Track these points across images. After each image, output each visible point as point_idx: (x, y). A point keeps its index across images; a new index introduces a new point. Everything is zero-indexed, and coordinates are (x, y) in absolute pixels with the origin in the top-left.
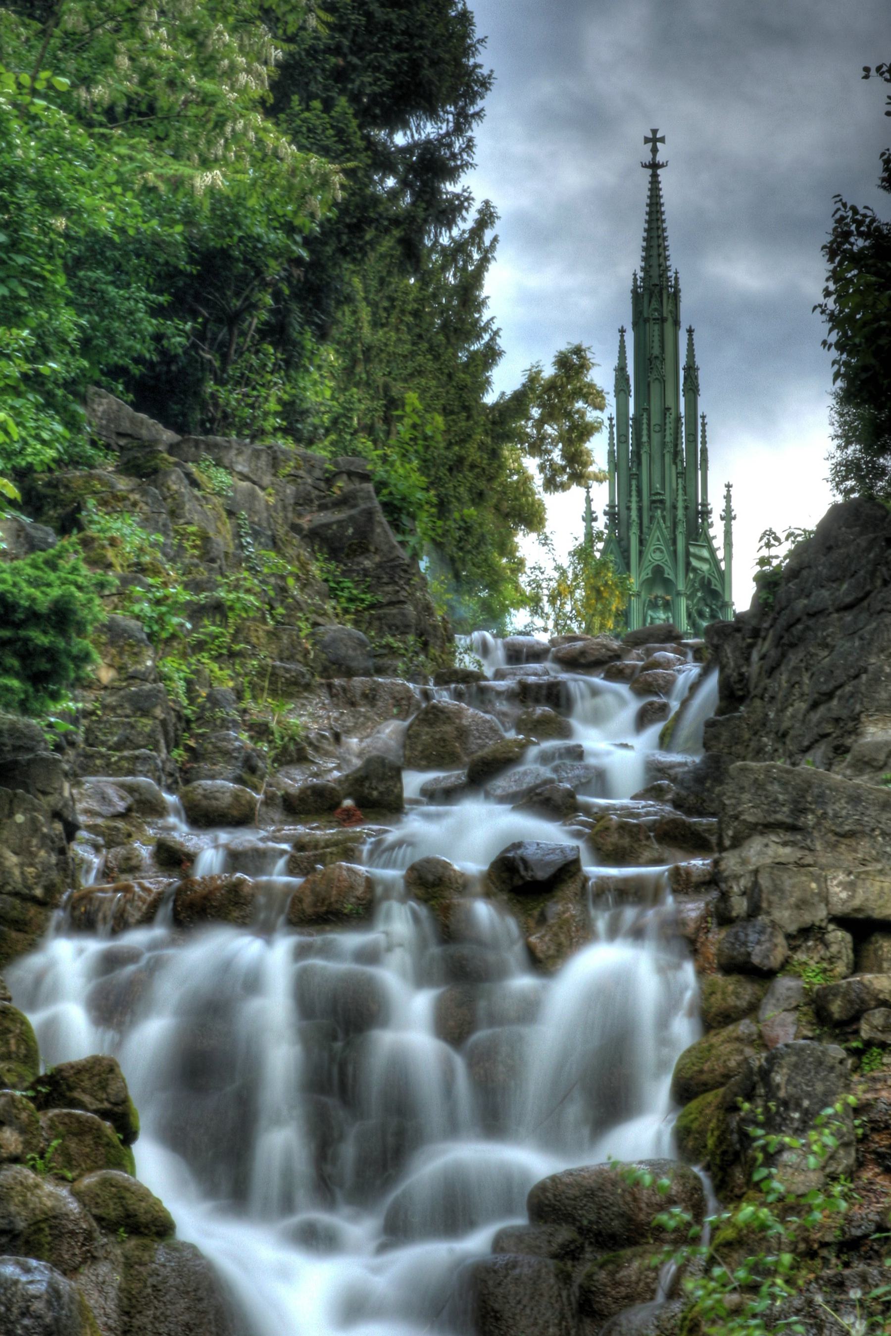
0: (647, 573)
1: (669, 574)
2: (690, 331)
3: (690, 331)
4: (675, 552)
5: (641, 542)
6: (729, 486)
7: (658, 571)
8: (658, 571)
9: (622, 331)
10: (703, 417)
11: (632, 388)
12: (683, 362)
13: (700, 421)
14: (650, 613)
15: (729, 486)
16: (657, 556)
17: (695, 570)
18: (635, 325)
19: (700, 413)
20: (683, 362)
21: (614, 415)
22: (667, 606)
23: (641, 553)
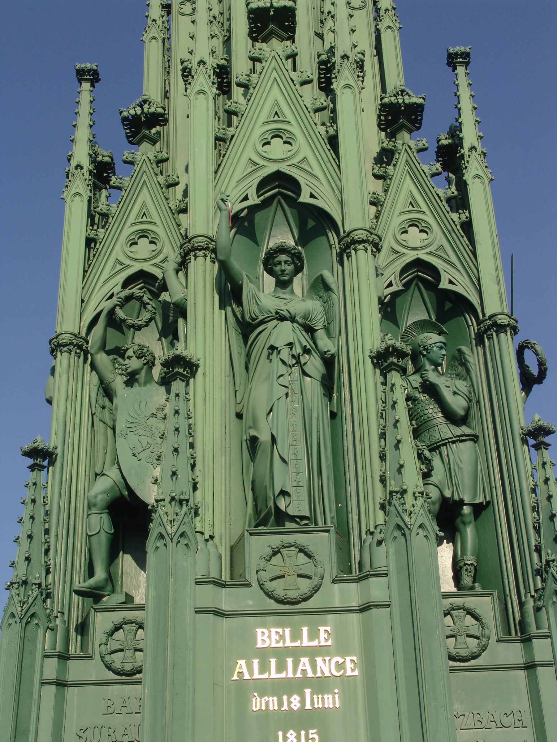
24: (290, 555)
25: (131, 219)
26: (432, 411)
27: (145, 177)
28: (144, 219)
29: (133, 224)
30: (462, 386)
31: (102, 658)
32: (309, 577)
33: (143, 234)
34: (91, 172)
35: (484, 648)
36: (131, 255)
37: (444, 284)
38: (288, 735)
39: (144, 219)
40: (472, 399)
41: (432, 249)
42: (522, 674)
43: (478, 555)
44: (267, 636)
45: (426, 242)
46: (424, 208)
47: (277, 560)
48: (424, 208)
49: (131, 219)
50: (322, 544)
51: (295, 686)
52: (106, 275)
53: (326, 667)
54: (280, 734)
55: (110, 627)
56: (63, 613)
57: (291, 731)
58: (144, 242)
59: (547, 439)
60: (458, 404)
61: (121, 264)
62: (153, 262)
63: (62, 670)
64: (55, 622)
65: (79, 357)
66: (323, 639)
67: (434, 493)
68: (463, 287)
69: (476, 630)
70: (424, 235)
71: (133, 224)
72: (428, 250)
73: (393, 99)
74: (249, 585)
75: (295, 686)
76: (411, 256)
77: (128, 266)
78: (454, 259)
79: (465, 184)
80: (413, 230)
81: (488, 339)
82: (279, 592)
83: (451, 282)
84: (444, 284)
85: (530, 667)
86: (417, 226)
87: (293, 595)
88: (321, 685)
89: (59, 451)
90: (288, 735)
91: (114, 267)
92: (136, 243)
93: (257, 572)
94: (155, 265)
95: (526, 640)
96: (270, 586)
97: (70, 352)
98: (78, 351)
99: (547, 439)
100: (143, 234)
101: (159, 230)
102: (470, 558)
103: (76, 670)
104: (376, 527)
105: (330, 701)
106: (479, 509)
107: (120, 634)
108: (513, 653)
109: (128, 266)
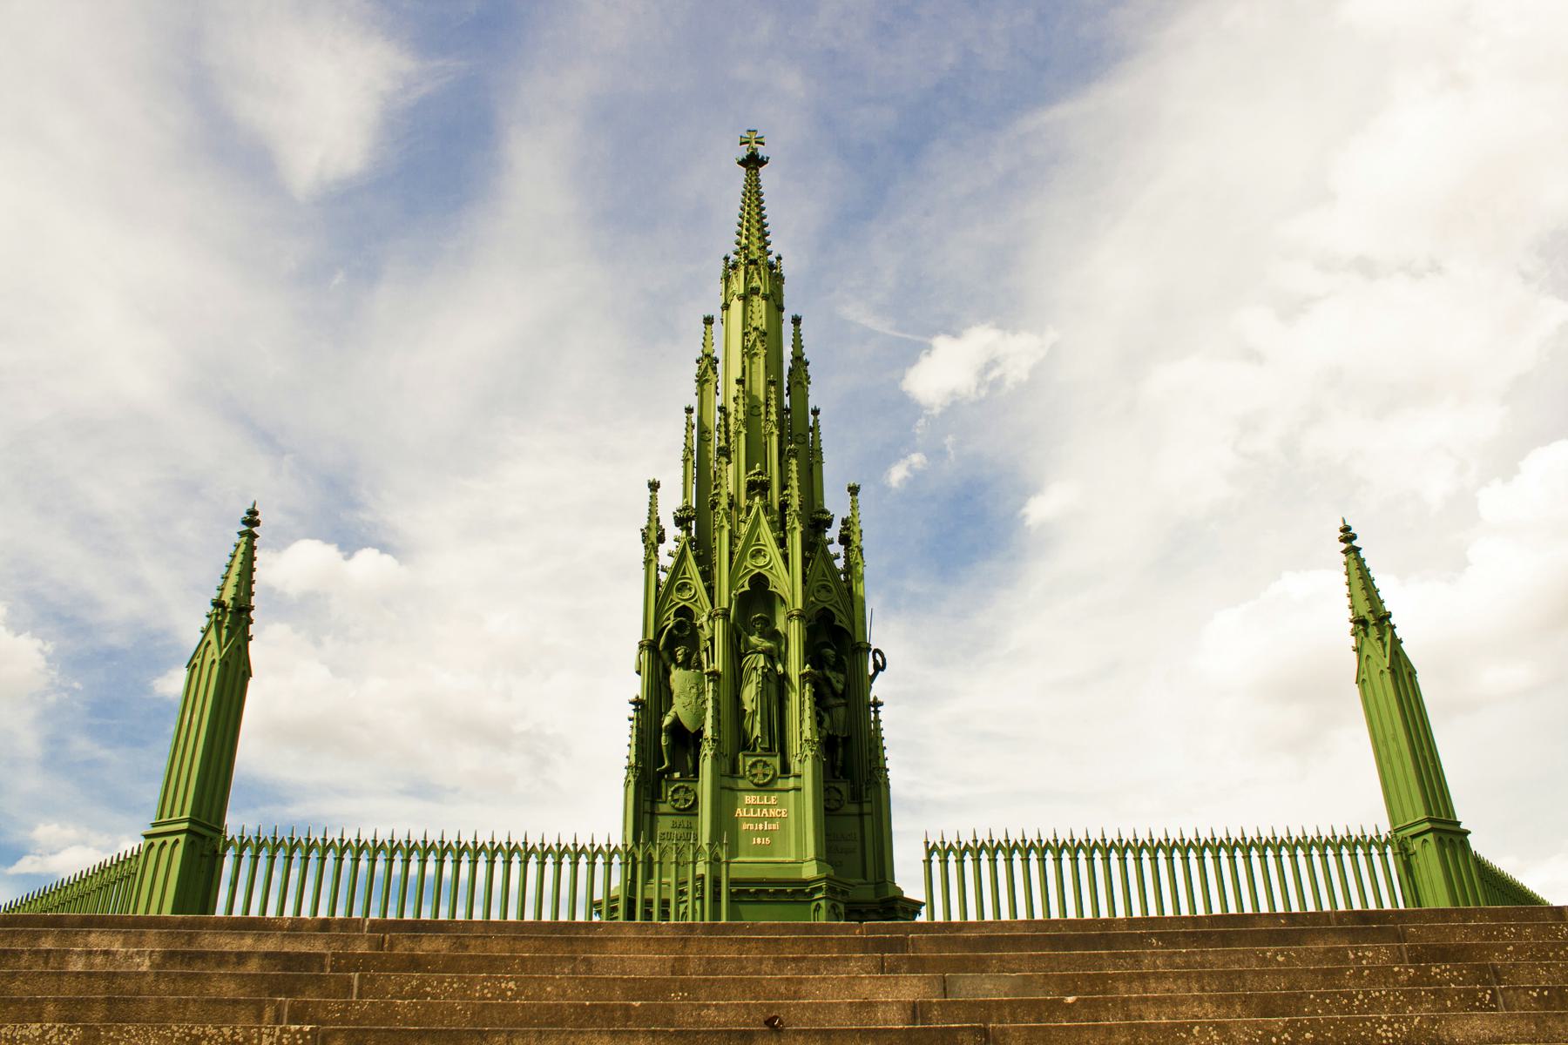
2: (796, 321)
3: (796, 321)
8: (759, 581)
10: (816, 412)
13: (811, 418)
15: (854, 490)
19: (811, 407)
26: (827, 690)
30: (841, 677)
37: (837, 623)
40: (846, 685)
43: (844, 761)
44: (749, 799)
51: (761, 819)
53: (773, 813)
60: (840, 687)
66: (772, 802)
67: (824, 733)
68: (845, 625)
75: (761, 819)
76: (821, 606)
84: (837, 623)
85: (861, 815)
88: (771, 820)
95: (861, 804)
101: (694, 583)
102: (839, 763)
105: (775, 826)
106: (847, 740)
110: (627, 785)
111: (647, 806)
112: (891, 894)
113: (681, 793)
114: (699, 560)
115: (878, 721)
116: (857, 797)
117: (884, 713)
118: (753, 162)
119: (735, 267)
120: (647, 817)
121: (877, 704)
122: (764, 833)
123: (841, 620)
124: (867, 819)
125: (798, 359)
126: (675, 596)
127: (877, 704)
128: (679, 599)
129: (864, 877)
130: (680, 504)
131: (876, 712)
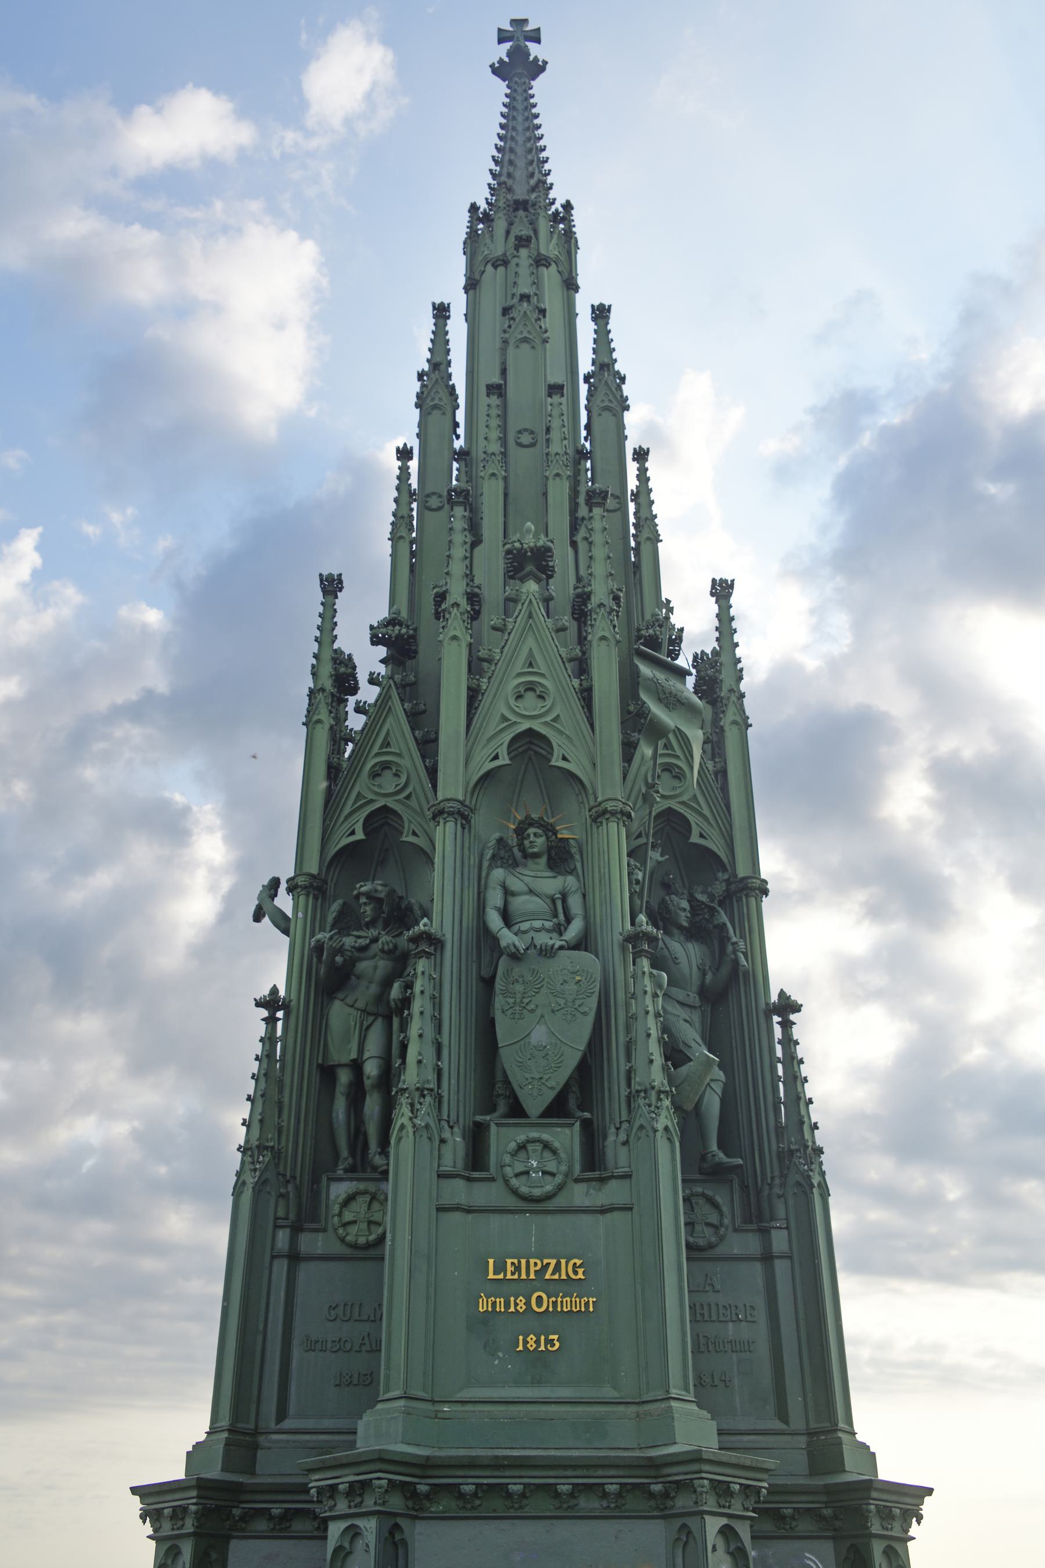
0: (493, 751)
1: (568, 753)
4: (586, 696)
5: (476, 665)
6: (722, 590)
7: (530, 745)
9: (441, 312)
10: (641, 455)
11: (462, 401)
12: (585, 365)
13: (632, 468)
14: (498, 873)
16: (530, 704)
17: (657, 732)
18: (471, 285)
20: (585, 365)
21: (414, 444)
22: (559, 857)
23: (474, 695)
24: (535, 1151)
25: (376, 749)
27: (390, 703)
28: (388, 750)
29: (377, 755)
31: (336, 1230)
32: (553, 1175)
33: (386, 766)
34: (332, 694)
35: (722, 1239)
36: (376, 789)
37: (695, 839)
38: (529, 1339)
39: (388, 750)
41: (685, 798)
42: (758, 1266)
45: (678, 791)
46: (679, 752)
47: (522, 1155)
48: (679, 752)
49: (376, 750)
50: (566, 1138)
52: (347, 810)
54: (521, 1338)
55: (343, 1196)
56: (294, 1178)
57: (532, 1336)
58: (388, 774)
59: (793, 1017)
61: (365, 798)
62: (397, 798)
63: (293, 1241)
64: (287, 1188)
65: (317, 899)
68: (715, 844)
69: (714, 1218)
70: (676, 783)
71: (377, 755)
72: (680, 799)
73: (651, 631)
74: (493, 1179)
76: (661, 805)
77: (371, 801)
78: (706, 811)
79: (722, 729)
80: (666, 776)
81: (737, 901)
82: (524, 1190)
83: (701, 836)
84: (695, 839)
86: (671, 772)
87: (537, 1192)
89: (293, 1004)
90: (529, 1339)
91: (355, 802)
92: (379, 775)
93: (502, 1167)
94: (397, 801)
96: (514, 1182)
97: (307, 895)
98: (316, 892)
99: (793, 1017)
100: (386, 766)
101: (405, 762)
103: (308, 1242)
104: (621, 1123)
107: (354, 1206)
108: (748, 1243)
109: (371, 801)
110: (238, 1191)
111: (283, 1237)
112: (853, 1472)
113: (359, 1206)
114: (414, 717)
115: (789, 1043)
116: (756, 1217)
117: (803, 1027)
118: (519, 64)
119: (487, 218)
120: (281, 1267)
121: (788, 1007)
122: (544, 1322)
123: (704, 833)
124: (781, 1267)
125: (605, 362)
126: (362, 785)
127: (788, 1007)
128: (368, 792)
129: (783, 1415)
130: (381, 612)
131: (787, 1025)
